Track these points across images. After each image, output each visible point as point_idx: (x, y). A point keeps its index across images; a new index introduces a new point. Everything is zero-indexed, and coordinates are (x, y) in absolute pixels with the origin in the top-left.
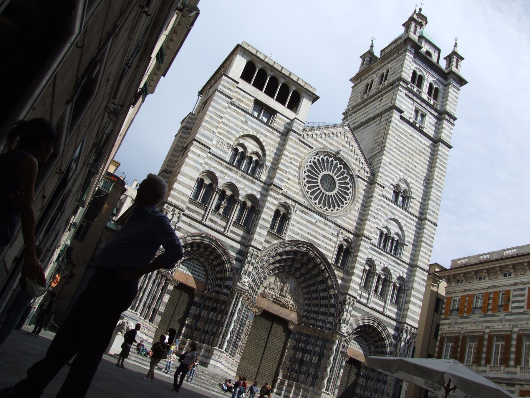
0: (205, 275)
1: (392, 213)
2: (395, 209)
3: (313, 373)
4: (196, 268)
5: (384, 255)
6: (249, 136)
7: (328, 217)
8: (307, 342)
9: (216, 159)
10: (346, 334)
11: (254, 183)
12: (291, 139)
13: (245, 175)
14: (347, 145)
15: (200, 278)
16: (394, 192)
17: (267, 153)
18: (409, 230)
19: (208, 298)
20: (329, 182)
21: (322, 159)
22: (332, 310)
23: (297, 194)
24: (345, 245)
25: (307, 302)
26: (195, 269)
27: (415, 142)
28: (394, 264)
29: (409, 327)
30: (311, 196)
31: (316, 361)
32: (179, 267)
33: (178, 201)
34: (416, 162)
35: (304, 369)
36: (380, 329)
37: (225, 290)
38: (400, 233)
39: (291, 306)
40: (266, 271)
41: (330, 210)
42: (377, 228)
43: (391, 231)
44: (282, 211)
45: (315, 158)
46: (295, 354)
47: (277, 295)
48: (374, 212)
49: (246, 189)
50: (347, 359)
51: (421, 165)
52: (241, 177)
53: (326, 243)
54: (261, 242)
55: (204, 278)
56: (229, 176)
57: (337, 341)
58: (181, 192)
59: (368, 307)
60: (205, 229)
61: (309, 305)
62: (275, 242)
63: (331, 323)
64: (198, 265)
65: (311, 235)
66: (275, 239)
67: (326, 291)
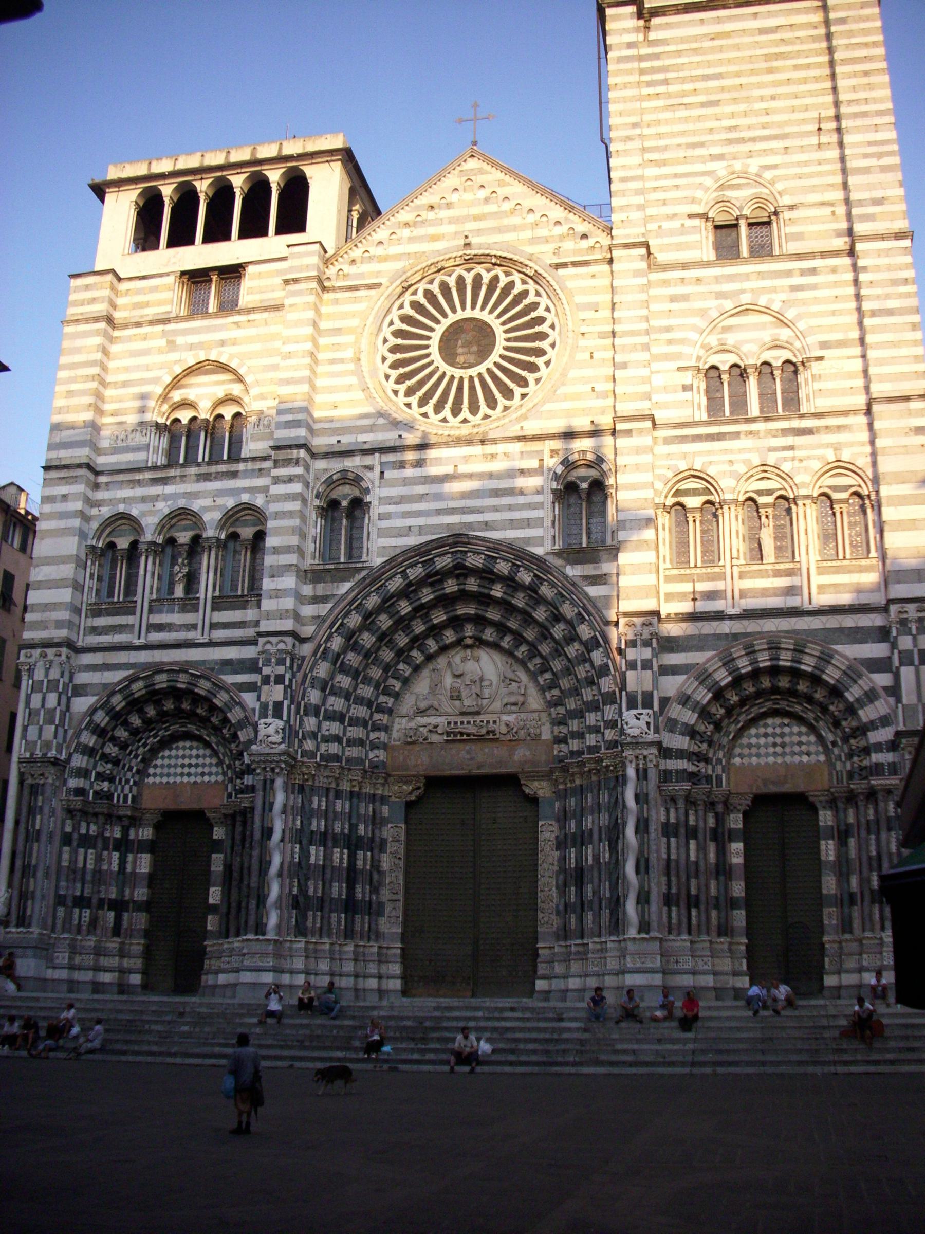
0: (217, 765)
1: (720, 295)
2: (731, 278)
3: (608, 895)
4: (190, 757)
5: (736, 435)
6: (191, 371)
7: (491, 435)
8: (578, 810)
9: (122, 477)
10: (651, 737)
11: (234, 475)
12: (291, 306)
13: (204, 469)
14: (492, 208)
15: (206, 778)
16: (717, 227)
17: (248, 379)
18: (814, 308)
19: (233, 816)
20: (470, 339)
21: (428, 294)
22: (606, 684)
23: (371, 429)
24: (584, 479)
25: (548, 695)
26: (187, 761)
27: (737, 47)
28: (790, 440)
29: (911, 607)
30: (423, 410)
31: (607, 855)
32: (149, 775)
33: (46, 628)
34: (762, 99)
35: (589, 889)
36: (808, 665)
37: (248, 780)
38: (785, 334)
39: (504, 730)
40: (376, 673)
41: (500, 407)
42: (679, 369)
43: (745, 348)
44: (345, 493)
45: (401, 307)
46: (563, 859)
48: (633, 333)
49: (220, 501)
50: (746, 802)
51: (787, 96)
52: (198, 481)
53: (510, 508)
54: (287, 611)
55: (217, 774)
56: (166, 497)
57: (631, 772)
58: (46, 605)
59: (731, 617)
60: (143, 657)
61: (558, 703)
62: (346, 586)
63: (612, 724)
64: (191, 748)
66: (344, 580)
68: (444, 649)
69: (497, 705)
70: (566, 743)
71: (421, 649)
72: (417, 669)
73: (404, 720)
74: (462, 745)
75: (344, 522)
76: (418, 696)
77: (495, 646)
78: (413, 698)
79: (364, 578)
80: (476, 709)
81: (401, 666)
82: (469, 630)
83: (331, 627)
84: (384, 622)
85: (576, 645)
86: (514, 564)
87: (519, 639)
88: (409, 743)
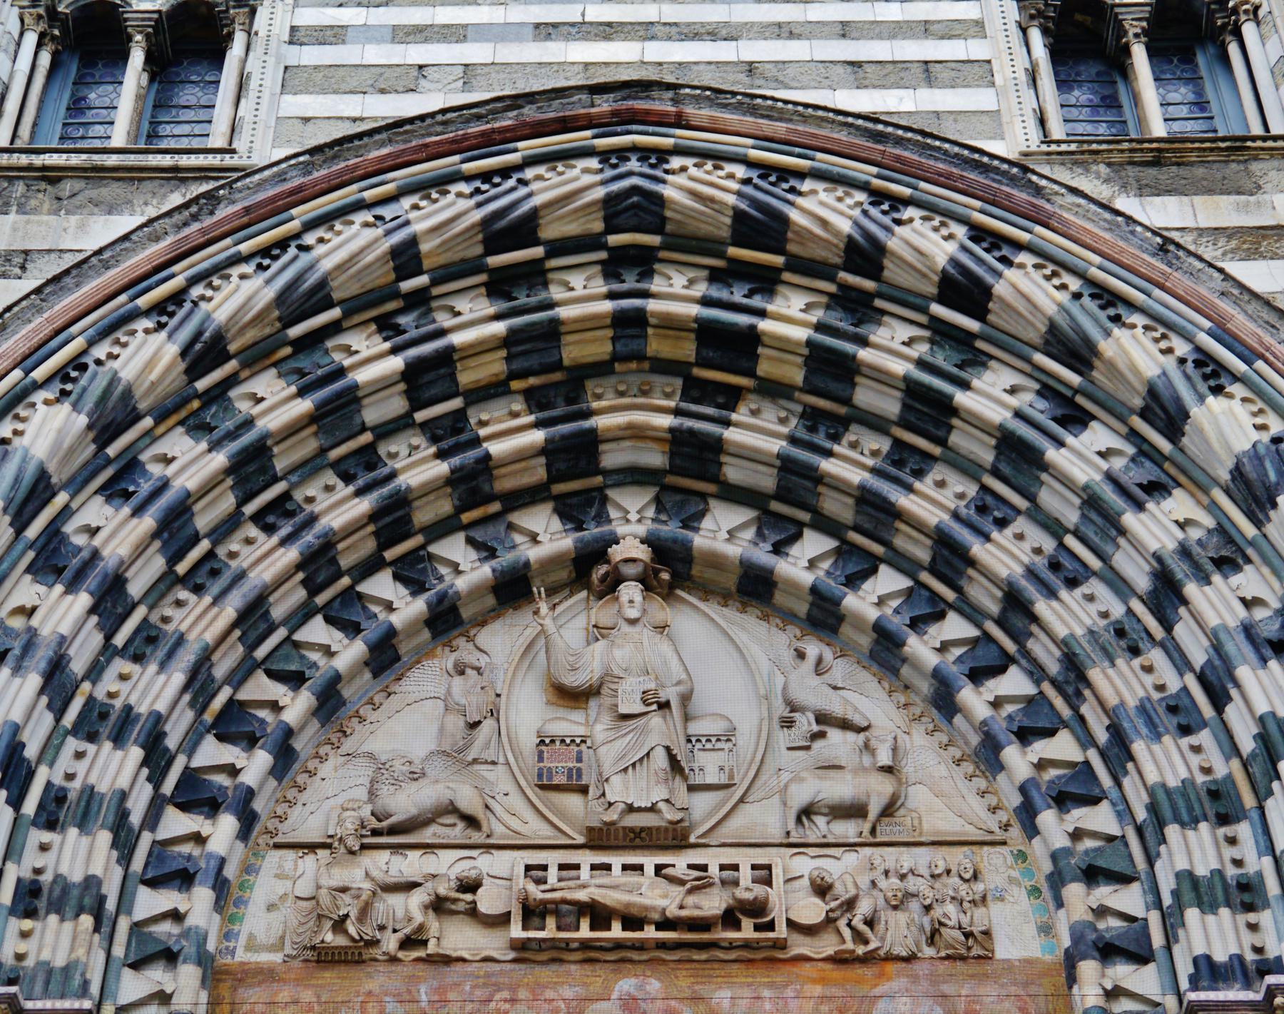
39: (811, 910)
40: (201, 620)
47: (553, 859)
65: (608, 31)
67: (1156, 489)
68: (513, 589)
69: (766, 817)
70: (1141, 957)
71: (413, 573)
72: (385, 657)
73: (309, 863)
74: (596, 977)
75: (137, 57)
76: (381, 766)
77: (755, 588)
78: (361, 774)
79: (211, 198)
80: (669, 814)
81: (317, 631)
82: (632, 523)
83: (29, 360)
84: (273, 402)
85: (1179, 504)
86: (878, 197)
87: (869, 531)
88: (324, 958)
